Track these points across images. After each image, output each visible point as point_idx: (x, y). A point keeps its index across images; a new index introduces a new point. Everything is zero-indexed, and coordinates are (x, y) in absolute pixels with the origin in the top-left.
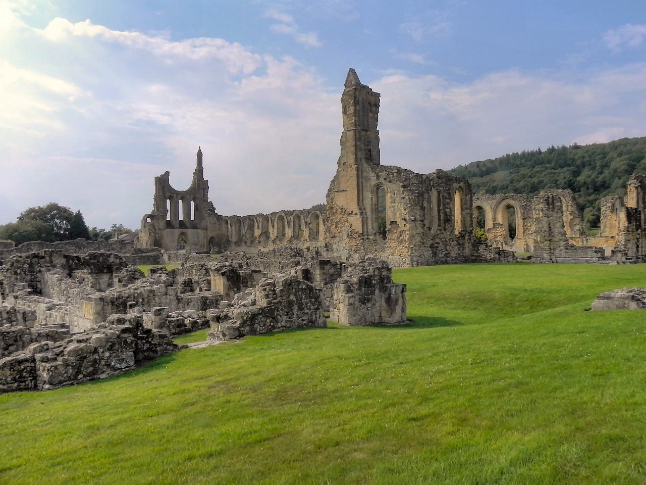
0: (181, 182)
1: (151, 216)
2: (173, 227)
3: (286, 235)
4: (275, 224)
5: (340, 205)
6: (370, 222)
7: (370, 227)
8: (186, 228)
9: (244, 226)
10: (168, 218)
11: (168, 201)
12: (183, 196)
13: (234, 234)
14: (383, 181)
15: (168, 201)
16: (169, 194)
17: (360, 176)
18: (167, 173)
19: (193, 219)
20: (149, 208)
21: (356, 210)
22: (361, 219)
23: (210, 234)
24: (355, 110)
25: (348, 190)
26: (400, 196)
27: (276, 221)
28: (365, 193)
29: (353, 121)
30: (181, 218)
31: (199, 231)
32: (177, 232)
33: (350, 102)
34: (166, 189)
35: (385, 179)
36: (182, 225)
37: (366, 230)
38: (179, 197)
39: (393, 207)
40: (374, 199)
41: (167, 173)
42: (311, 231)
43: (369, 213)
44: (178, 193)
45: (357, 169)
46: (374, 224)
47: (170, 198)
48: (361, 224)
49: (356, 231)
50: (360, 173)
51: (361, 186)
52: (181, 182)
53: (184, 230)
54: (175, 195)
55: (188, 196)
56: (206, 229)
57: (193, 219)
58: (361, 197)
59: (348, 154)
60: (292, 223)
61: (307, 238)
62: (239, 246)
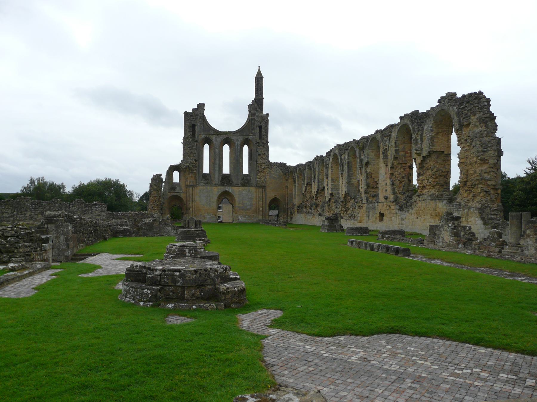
0: (227, 118)
11: (206, 148)
12: (227, 138)
13: (296, 193)
15: (206, 148)
16: (203, 136)
18: (201, 106)
19: (246, 170)
20: (177, 157)
23: (271, 195)
31: (252, 189)
32: (216, 191)
36: (226, 179)
41: (201, 106)
47: (208, 141)
52: (227, 118)
54: (213, 138)
56: (263, 187)
57: (246, 170)
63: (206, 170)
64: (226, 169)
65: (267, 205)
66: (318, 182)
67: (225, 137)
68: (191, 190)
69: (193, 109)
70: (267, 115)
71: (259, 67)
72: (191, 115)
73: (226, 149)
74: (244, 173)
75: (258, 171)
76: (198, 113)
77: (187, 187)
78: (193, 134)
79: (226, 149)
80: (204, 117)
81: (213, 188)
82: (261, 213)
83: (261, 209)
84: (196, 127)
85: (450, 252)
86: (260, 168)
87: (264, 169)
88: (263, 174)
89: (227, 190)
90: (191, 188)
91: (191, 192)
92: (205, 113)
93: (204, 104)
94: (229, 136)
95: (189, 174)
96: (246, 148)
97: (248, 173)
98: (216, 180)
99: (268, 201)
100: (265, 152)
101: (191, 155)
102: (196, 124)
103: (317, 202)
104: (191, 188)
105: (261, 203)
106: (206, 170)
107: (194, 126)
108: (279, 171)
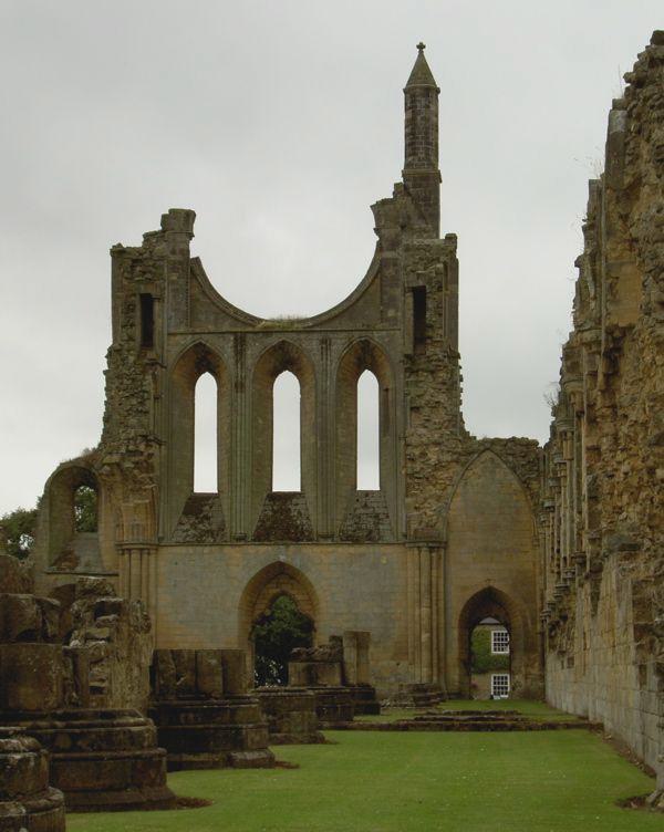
12: (283, 346)
15: (206, 389)
18: (179, 223)
19: (368, 477)
23: (468, 575)
34: (164, 316)
38: (254, 350)
41: (179, 223)
44: (244, 327)
47: (203, 360)
54: (226, 349)
55: (312, 344)
56: (434, 544)
57: (368, 477)
63: (206, 479)
64: (287, 476)
65: (454, 621)
67: (274, 340)
68: (135, 562)
69: (148, 237)
70: (452, 238)
71: (421, 47)
72: (135, 261)
73: (287, 388)
74: (362, 486)
75: (411, 476)
76: (161, 248)
77: (123, 549)
78: (148, 338)
79: (287, 388)
80: (194, 269)
81: (227, 550)
82: (425, 655)
83: (425, 637)
84: (157, 307)
85: (553, 548)
86: (418, 466)
87: (438, 466)
88: (432, 490)
89: (282, 558)
90: (135, 555)
91: (135, 571)
92: (196, 249)
93: (189, 216)
94: (288, 338)
95: (126, 499)
96: (368, 385)
97: (377, 487)
98: (245, 518)
99: (457, 605)
100: (442, 398)
101: (133, 421)
102: (158, 292)
104: (135, 555)
105: (425, 611)
106: (206, 479)
107: (148, 302)
108: (504, 474)
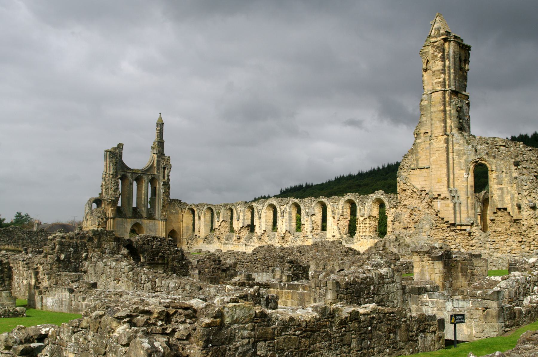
1: (98, 202)
2: (124, 216)
3: (279, 230)
4: (263, 215)
5: (419, 187)
6: (463, 208)
7: (464, 216)
8: (141, 217)
9: (218, 217)
10: (119, 205)
12: (138, 176)
14: (485, 157)
17: (451, 150)
21: (445, 193)
22: (452, 205)
24: (444, 66)
25: (433, 167)
26: (510, 176)
27: (264, 210)
28: (457, 172)
29: (441, 80)
30: (134, 205)
33: (436, 56)
35: (487, 154)
37: (458, 219)
39: (500, 189)
40: (469, 179)
42: (315, 225)
43: (463, 198)
44: (134, 172)
45: (447, 141)
46: (470, 212)
47: (123, 178)
48: (452, 212)
49: (445, 220)
50: (450, 146)
51: (451, 162)
53: (138, 221)
54: (129, 175)
58: (451, 176)
59: (433, 122)
60: (287, 214)
61: (309, 233)
62: (209, 243)
66: (244, 220)
95: (111, 207)
103: (241, 235)
